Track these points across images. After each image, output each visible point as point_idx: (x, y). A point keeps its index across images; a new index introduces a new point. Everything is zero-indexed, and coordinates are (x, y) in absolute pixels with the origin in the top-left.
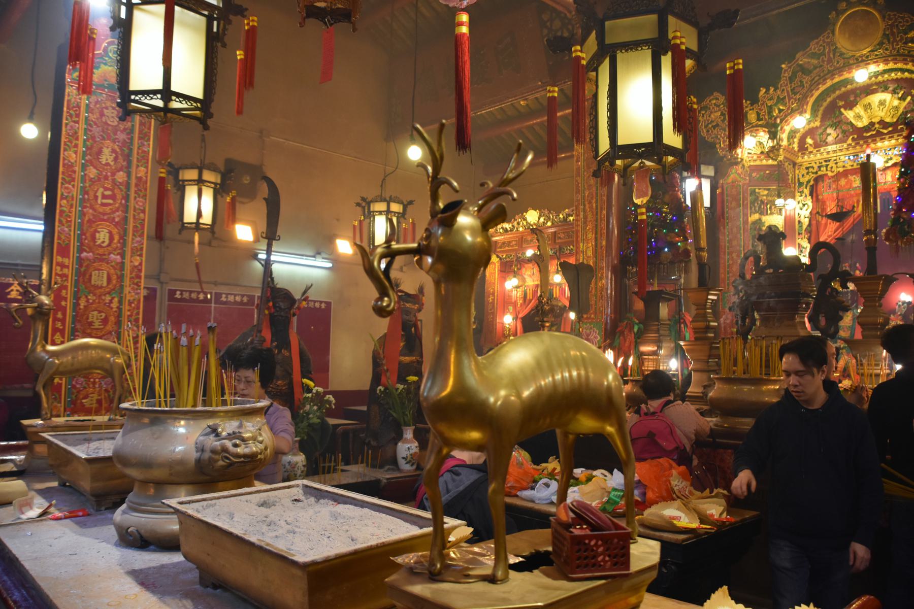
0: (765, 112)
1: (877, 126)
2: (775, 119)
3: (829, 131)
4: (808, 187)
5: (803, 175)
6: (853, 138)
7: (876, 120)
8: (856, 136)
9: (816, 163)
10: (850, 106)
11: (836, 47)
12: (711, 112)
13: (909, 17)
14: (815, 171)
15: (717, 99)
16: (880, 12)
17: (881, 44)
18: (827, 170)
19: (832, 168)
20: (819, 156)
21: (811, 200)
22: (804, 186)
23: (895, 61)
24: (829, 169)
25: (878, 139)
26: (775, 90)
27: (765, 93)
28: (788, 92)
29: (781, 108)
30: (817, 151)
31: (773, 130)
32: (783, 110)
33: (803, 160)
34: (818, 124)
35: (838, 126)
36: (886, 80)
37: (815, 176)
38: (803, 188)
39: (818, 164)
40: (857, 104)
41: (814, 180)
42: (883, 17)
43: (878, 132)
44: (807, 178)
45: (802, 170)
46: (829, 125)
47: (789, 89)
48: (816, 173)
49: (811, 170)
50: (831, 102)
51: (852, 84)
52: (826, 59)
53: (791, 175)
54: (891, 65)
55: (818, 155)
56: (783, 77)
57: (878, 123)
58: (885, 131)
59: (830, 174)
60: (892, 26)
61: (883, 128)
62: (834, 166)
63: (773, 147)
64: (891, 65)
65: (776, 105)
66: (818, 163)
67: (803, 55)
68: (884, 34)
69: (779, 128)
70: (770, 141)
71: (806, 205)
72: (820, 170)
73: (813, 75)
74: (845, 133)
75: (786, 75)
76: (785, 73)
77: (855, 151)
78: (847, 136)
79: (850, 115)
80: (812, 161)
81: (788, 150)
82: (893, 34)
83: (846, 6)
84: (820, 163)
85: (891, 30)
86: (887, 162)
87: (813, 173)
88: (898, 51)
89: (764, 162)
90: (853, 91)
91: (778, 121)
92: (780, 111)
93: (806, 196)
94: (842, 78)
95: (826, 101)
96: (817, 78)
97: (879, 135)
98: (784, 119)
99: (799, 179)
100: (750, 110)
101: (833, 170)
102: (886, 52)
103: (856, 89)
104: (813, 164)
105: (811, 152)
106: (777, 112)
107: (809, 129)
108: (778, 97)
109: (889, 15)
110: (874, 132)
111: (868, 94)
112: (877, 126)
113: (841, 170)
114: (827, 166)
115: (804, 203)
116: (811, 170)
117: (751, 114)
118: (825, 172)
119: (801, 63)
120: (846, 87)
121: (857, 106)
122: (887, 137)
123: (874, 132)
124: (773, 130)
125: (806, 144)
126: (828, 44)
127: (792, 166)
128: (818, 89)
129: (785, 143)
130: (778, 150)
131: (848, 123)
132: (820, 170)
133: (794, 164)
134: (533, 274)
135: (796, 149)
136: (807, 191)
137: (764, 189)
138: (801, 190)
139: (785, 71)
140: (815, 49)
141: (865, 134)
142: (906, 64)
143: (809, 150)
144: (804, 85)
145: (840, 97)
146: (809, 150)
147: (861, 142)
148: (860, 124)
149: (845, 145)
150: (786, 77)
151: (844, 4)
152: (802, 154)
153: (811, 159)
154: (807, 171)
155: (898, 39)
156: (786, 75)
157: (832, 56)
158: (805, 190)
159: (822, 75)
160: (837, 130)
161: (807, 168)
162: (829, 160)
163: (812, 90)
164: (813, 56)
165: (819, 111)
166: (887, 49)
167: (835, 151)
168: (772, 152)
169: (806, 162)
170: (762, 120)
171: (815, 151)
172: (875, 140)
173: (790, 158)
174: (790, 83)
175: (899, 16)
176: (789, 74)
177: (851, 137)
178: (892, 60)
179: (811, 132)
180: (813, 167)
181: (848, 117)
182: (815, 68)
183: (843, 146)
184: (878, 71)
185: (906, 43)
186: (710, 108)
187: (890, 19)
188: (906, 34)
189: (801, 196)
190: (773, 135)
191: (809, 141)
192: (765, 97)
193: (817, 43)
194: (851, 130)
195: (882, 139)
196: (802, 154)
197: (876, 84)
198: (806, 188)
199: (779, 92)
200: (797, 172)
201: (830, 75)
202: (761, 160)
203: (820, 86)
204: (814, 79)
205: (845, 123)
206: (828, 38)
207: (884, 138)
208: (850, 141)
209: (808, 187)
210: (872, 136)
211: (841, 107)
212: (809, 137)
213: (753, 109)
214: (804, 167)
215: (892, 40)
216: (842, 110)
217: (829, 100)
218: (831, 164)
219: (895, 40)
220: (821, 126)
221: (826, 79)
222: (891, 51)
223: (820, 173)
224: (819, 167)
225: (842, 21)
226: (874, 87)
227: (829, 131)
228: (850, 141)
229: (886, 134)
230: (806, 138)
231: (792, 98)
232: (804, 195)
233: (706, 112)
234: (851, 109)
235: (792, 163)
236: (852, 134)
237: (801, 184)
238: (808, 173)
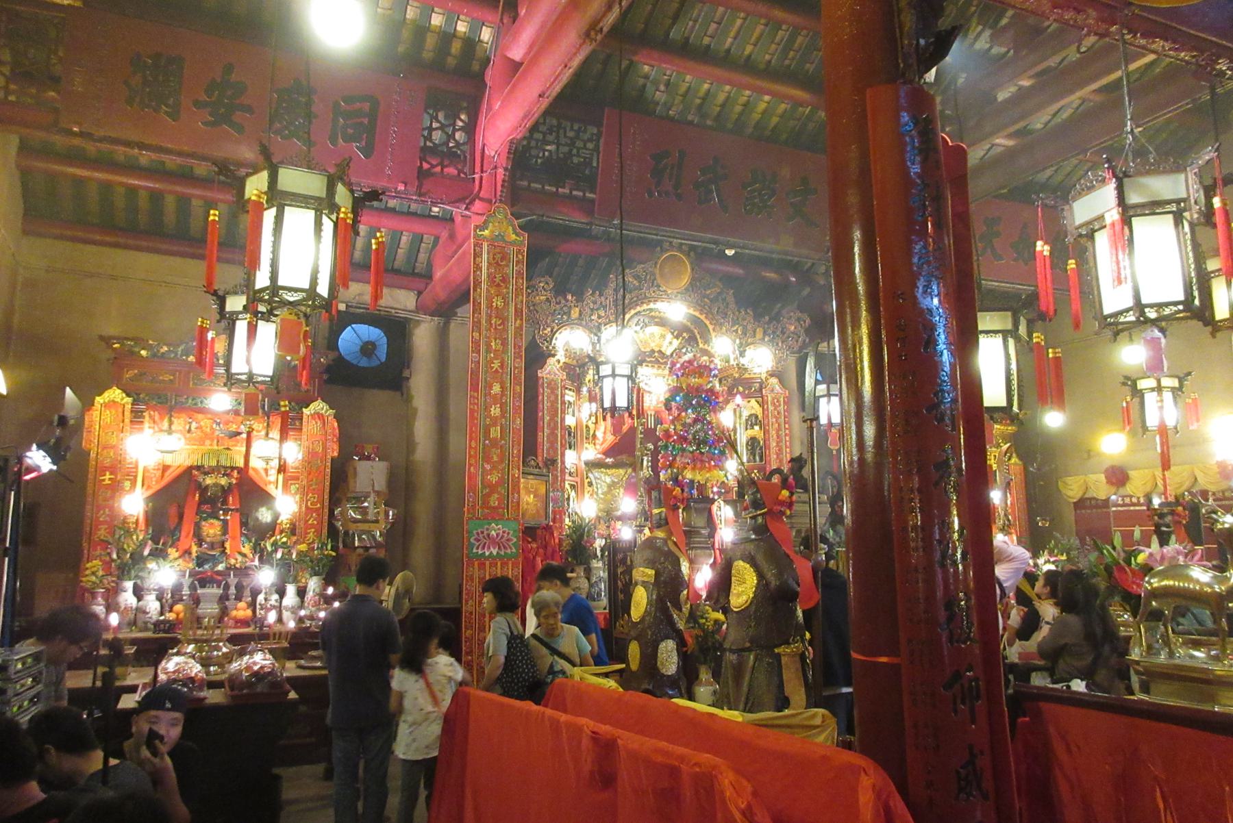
1: (656, 354)
11: (655, 279)
12: (538, 295)
15: (547, 283)
16: (691, 263)
17: (687, 289)
25: (656, 366)
26: (601, 295)
65: (597, 310)
73: (633, 295)
96: (635, 299)
108: (601, 303)
112: (656, 354)
134: (189, 431)
142: (701, 314)
164: (637, 277)
182: (635, 290)
186: (537, 290)
193: (643, 268)
199: (603, 298)
201: (646, 301)
204: (632, 298)
206: (651, 267)
210: (651, 362)
219: (696, 292)
221: (642, 303)
229: (662, 364)
233: (533, 291)
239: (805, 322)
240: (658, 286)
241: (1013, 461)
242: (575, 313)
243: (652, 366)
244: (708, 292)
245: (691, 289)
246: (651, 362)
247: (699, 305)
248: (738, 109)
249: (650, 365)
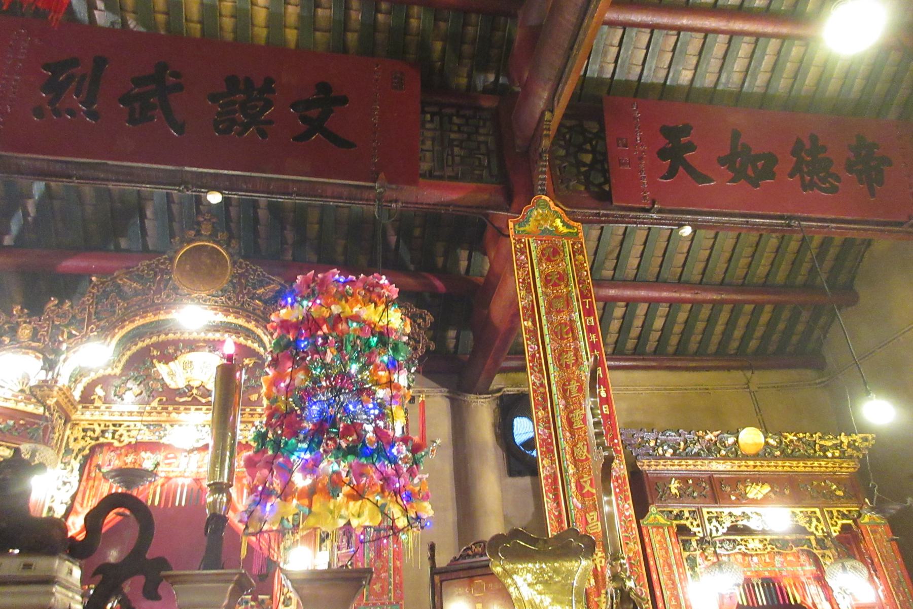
0: (47, 331)
1: (195, 391)
2: (60, 343)
3: (130, 384)
4: (80, 457)
5: (76, 439)
6: (160, 400)
7: (195, 384)
8: (164, 399)
9: (100, 425)
10: (167, 358)
11: (171, 278)
13: (261, 272)
14: (96, 435)
16: (231, 255)
18: (113, 438)
19: (121, 436)
20: (106, 417)
21: (78, 478)
22: (74, 455)
23: (237, 314)
24: (116, 436)
25: (193, 408)
27: (56, 305)
28: (90, 313)
29: (74, 332)
30: (107, 408)
31: (52, 357)
32: (76, 336)
33: (83, 417)
34: (118, 371)
35: (144, 380)
36: (216, 339)
37: (93, 443)
38: (70, 458)
39: (102, 427)
40: (176, 358)
41: (90, 449)
42: (234, 263)
43: (195, 399)
44: (82, 444)
45: (75, 432)
46: (132, 377)
47: (92, 311)
48: (97, 439)
49: (90, 433)
50: (142, 349)
51: (175, 334)
52: (154, 288)
53: (57, 434)
54: (231, 319)
55: (107, 413)
56: (90, 292)
57: (197, 388)
58: (204, 401)
59: (116, 444)
60: (241, 275)
61: (201, 396)
62: (125, 434)
63: (45, 381)
64: (231, 319)
65: (67, 326)
66: (102, 426)
67: (126, 274)
68: (231, 281)
69: (62, 358)
70: (44, 372)
71: (68, 484)
72: (103, 436)
74: (151, 392)
75: (95, 291)
76: (93, 288)
77: (159, 419)
78: (153, 396)
79: (162, 369)
80: (95, 421)
81: (66, 393)
82: (240, 283)
83: (195, 236)
84: (105, 426)
85: (240, 279)
86: (198, 441)
87: (92, 439)
88: (242, 305)
89: (21, 407)
90: (175, 343)
91: (64, 347)
92: (70, 334)
93: (72, 470)
94: (169, 317)
95: (136, 345)
97: (195, 402)
98: (72, 348)
99: (67, 443)
100: (25, 322)
101: (122, 439)
102: (229, 302)
103: (179, 341)
104: (96, 427)
105: (96, 408)
106: (65, 336)
107: (104, 376)
109: (241, 263)
110: (190, 399)
111: (192, 350)
113: (133, 441)
114: (114, 433)
115: (66, 480)
116: (90, 433)
117: (25, 328)
118: (110, 440)
119: (119, 282)
120: (167, 334)
121: (176, 361)
122: (204, 408)
123: (190, 399)
124: (52, 357)
125: (93, 395)
126: (162, 271)
127: (63, 421)
128: (133, 321)
129: (63, 381)
130: (51, 388)
131: (158, 380)
132: (103, 436)
133: (67, 420)
135: (77, 398)
136: (76, 464)
137: (8, 447)
138: (66, 461)
139: (95, 285)
140: (143, 271)
141: (177, 399)
142: (249, 322)
143: (96, 404)
144: (115, 311)
145: (156, 346)
146: (96, 404)
147: (171, 408)
148: (173, 385)
149: (148, 408)
150: (93, 293)
151: (192, 233)
152: (83, 407)
153: (95, 418)
154: (83, 434)
155: (245, 292)
156: (95, 291)
157: (162, 286)
158: (73, 461)
159: (143, 305)
160: (142, 385)
161: (84, 430)
162: (120, 425)
163: (125, 321)
165: (124, 355)
166: (230, 299)
167: (131, 413)
168: (38, 393)
169: (87, 420)
170: (39, 341)
171: (103, 407)
172: (189, 409)
173: (65, 407)
174: (97, 304)
175: (251, 268)
176: (98, 291)
177: (158, 399)
178: (233, 312)
179: (103, 381)
180: (94, 431)
181: (160, 371)
183: (145, 408)
184: (214, 322)
185: (252, 298)
187: (241, 267)
188: (255, 288)
189: (65, 469)
190: (50, 366)
191: (99, 391)
192: (54, 311)
193: (148, 266)
194: (161, 390)
195: (197, 409)
196: (83, 407)
197: (205, 341)
198: (75, 459)
200: (68, 432)
202: (17, 402)
203: (138, 318)
205: (155, 379)
206: (162, 263)
207: (201, 409)
208: (155, 404)
209: (80, 457)
210: (184, 403)
211: (154, 357)
212: (100, 386)
213: (30, 323)
214: (80, 429)
215: (238, 290)
216: (154, 361)
217: (141, 345)
218: (121, 430)
219: (241, 292)
220: (121, 375)
221: (147, 312)
222: (234, 302)
223: (102, 440)
224: (103, 432)
225: (186, 252)
226: (201, 344)
227: (130, 384)
228: (155, 404)
230: (96, 386)
231: (94, 323)
232: (69, 468)
234: (167, 363)
235: (63, 417)
236: (160, 394)
237: (68, 451)
238: (83, 438)
239: (424, 320)
240: (175, 289)
241: (866, 519)
242: (25, 332)
243: (186, 409)
244: (261, 291)
245: (230, 288)
246: (184, 403)
247: (246, 310)
248: (228, 23)
249: (182, 408)
